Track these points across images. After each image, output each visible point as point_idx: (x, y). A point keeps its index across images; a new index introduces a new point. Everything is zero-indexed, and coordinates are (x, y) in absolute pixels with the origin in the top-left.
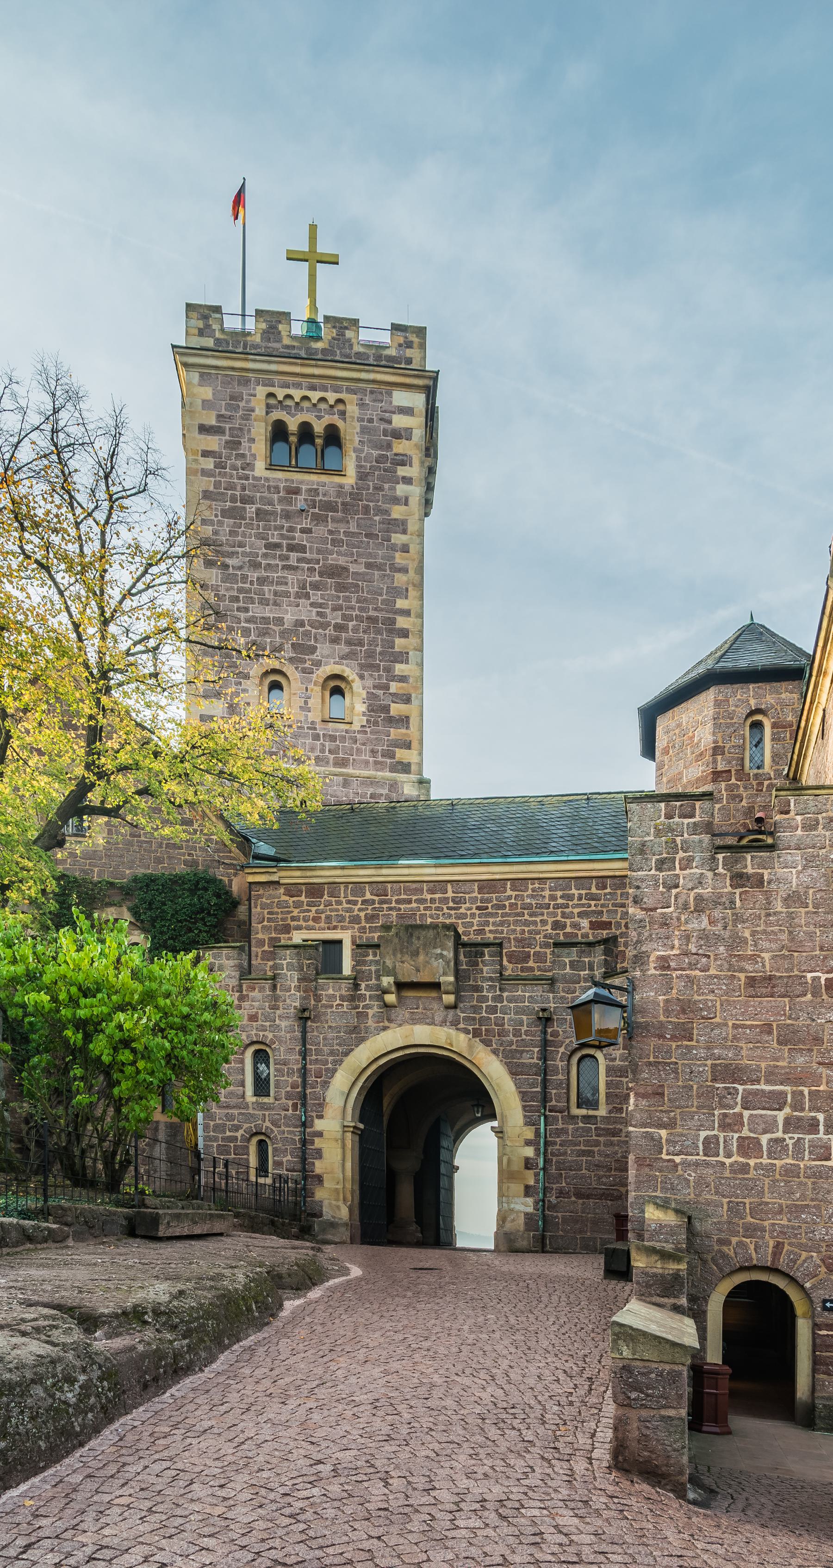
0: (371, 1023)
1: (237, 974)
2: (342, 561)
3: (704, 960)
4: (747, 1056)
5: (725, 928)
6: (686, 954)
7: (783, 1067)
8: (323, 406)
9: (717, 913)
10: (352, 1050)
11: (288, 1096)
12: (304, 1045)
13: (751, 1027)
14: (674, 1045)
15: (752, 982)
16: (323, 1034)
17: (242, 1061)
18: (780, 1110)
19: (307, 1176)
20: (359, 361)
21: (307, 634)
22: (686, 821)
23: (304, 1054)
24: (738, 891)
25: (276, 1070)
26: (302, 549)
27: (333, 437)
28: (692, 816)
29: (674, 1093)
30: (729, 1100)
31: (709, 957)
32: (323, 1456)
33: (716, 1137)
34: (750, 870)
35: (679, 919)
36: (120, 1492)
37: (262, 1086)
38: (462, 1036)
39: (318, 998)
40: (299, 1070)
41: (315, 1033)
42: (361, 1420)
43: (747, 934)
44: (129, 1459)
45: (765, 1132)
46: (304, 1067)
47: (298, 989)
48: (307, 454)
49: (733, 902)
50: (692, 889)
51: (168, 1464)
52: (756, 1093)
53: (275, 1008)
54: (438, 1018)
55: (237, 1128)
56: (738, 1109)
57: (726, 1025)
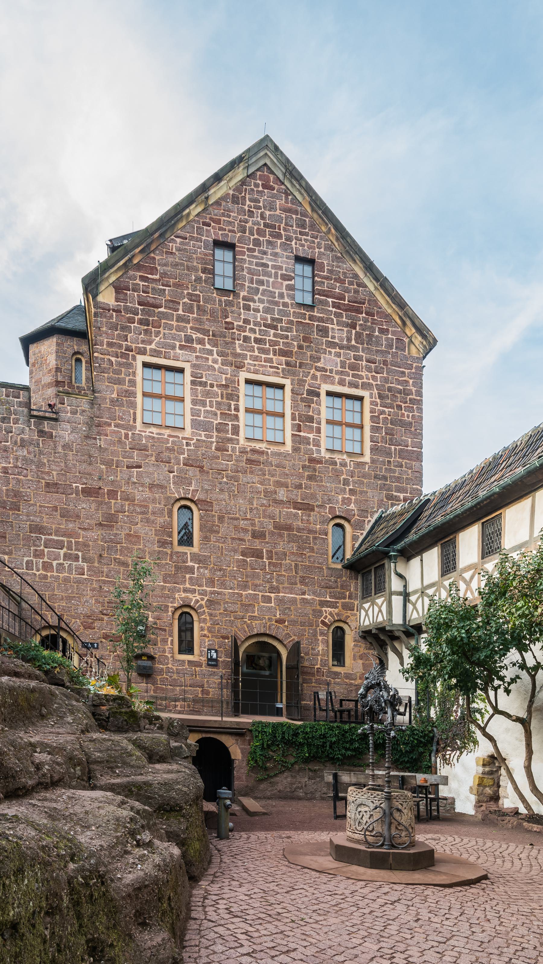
3: (25, 471)
4: (46, 521)
5: (35, 456)
6: (16, 467)
7: (63, 529)
9: (31, 449)
13: (48, 507)
14: (11, 513)
15: (48, 485)
18: (61, 549)
22: (16, 400)
24: (41, 439)
28: (19, 398)
29: (11, 537)
30: (37, 543)
31: (27, 470)
33: (32, 561)
34: (46, 429)
35: (13, 449)
43: (45, 461)
45: (55, 560)
49: (38, 444)
50: (19, 435)
52: (50, 540)
56: (42, 548)
57: (36, 505)
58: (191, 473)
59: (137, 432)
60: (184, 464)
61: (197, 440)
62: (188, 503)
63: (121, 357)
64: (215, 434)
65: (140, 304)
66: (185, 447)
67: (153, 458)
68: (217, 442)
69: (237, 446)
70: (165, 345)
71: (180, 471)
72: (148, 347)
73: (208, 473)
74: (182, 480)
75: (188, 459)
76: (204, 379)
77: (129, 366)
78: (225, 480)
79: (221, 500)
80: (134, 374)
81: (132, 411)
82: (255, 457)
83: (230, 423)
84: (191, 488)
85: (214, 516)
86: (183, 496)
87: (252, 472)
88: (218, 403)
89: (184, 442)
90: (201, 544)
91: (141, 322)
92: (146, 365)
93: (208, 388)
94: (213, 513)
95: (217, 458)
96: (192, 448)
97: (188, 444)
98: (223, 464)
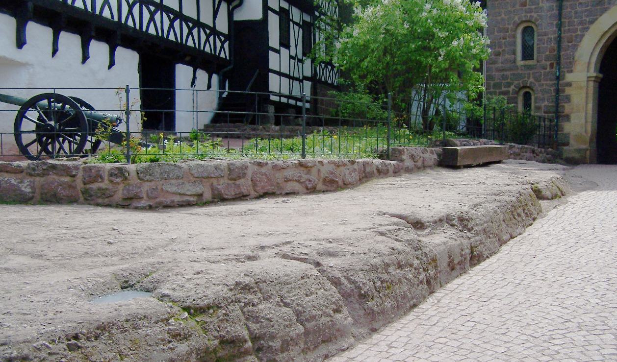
10: (597, 19)
11: (547, 58)
12: (560, 19)
17: (514, 37)
19: (558, 114)
23: (560, 26)
25: (539, 40)
32: (571, 317)
36: (440, 335)
37: (528, 53)
40: (555, 38)
41: (569, 10)
42: (598, 293)
44: (444, 315)
46: (560, 36)
51: (468, 318)
55: (509, 85)
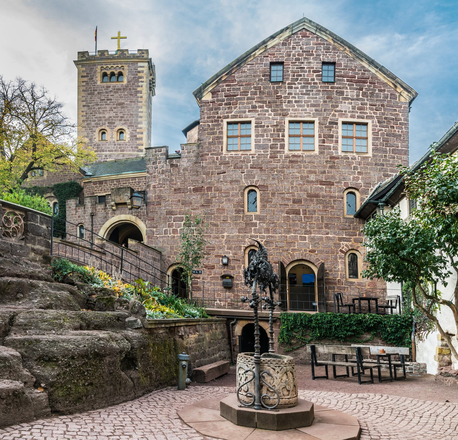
0: (110, 215)
1: (75, 206)
2: (123, 101)
8: (117, 68)
16: (97, 220)
20: (129, 58)
21: (112, 120)
26: (111, 100)
27: (121, 74)
34: (175, 163)
38: (134, 217)
39: (96, 210)
47: (91, 208)
48: (114, 78)
49: (170, 171)
53: (85, 213)
54: (127, 212)
58: (254, 172)
59: (223, 155)
60: (250, 168)
61: (258, 154)
62: (254, 188)
63: (215, 122)
64: (270, 150)
65: (225, 96)
66: (251, 159)
67: (233, 167)
68: (271, 154)
69: (283, 155)
70: (239, 112)
71: (248, 171)
72: (230, 115)
73: (265, 170)
74: (250, 176)
75: (253, 165)
76: (263, 124)
77: (219, 125)
78: (276, 173)
79: (273, 184)
80: (222, 128)
81: (220, 146)
82: (295, 159)
83: (279, 144)
84: (255, 180)
85: (269, 193)
86: (250, 184)
87: (292, 167)
88: (271, 134)
89: (251, 156)
90: (261, 209)
91: (226, 104)
92: (229, 123)
93: (266, 128)
94: (268, 192)
95: (271, 162)
96: (256, 159)
97: (252, 157)
98: (274, 165)
